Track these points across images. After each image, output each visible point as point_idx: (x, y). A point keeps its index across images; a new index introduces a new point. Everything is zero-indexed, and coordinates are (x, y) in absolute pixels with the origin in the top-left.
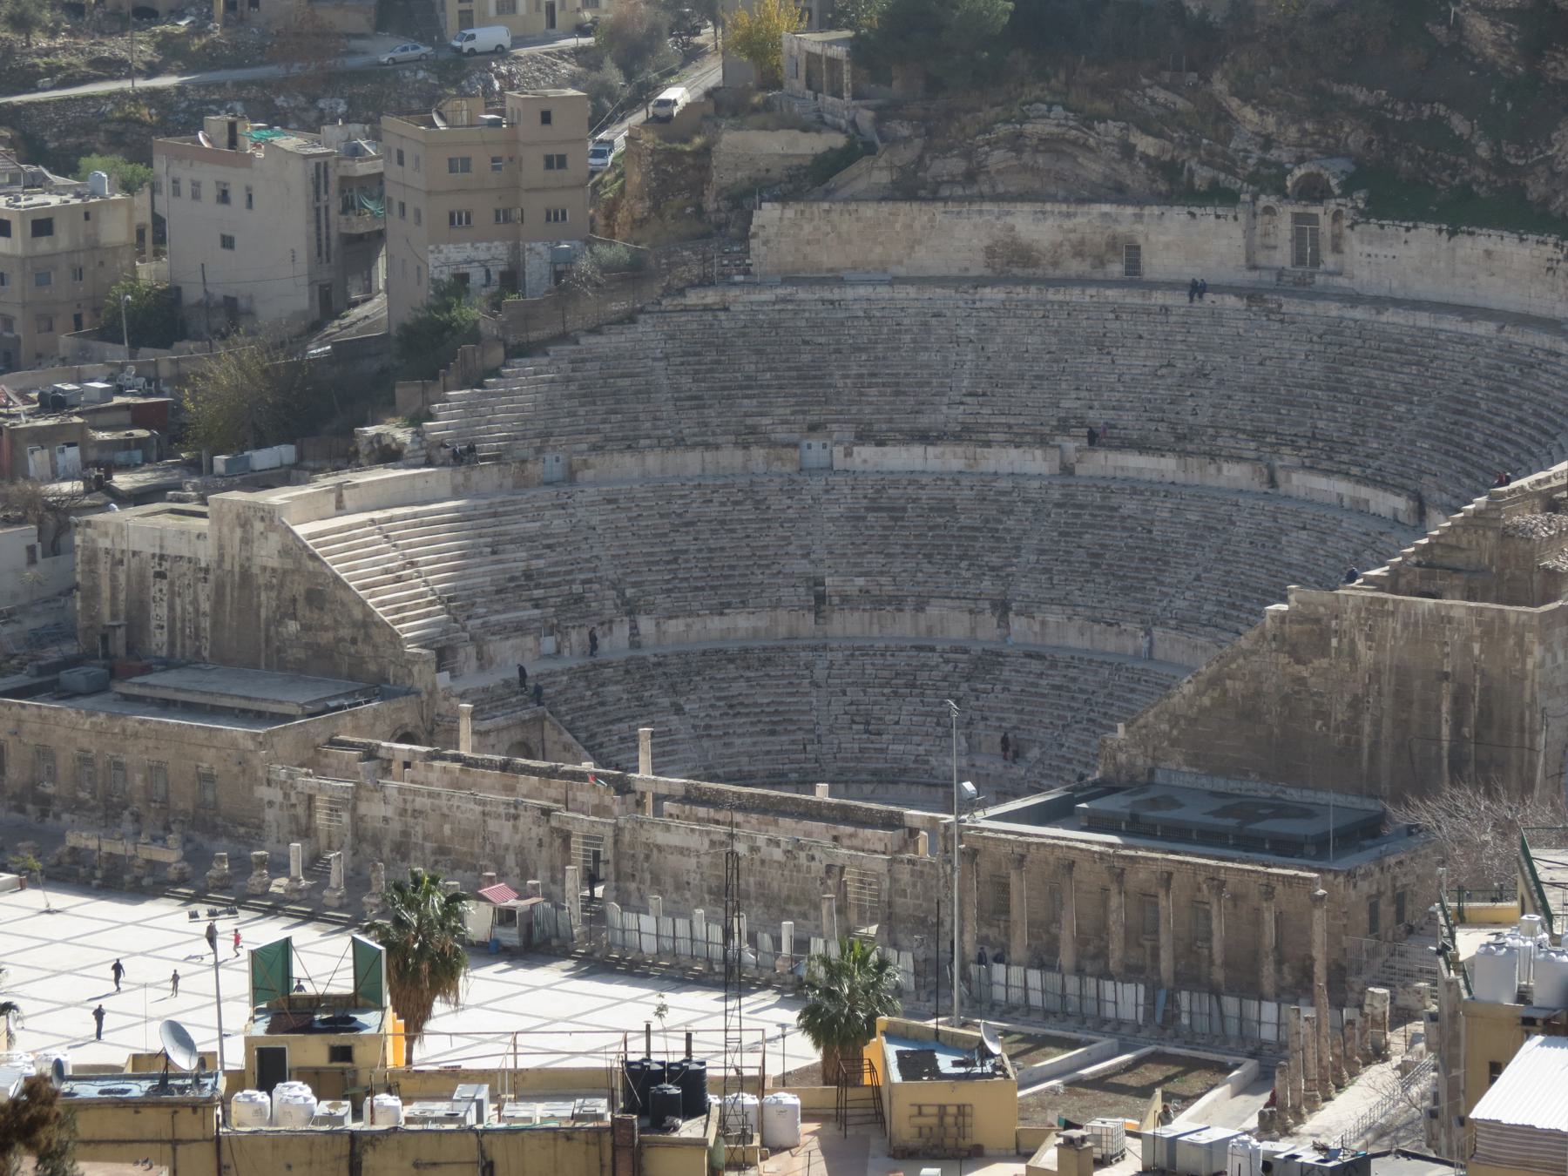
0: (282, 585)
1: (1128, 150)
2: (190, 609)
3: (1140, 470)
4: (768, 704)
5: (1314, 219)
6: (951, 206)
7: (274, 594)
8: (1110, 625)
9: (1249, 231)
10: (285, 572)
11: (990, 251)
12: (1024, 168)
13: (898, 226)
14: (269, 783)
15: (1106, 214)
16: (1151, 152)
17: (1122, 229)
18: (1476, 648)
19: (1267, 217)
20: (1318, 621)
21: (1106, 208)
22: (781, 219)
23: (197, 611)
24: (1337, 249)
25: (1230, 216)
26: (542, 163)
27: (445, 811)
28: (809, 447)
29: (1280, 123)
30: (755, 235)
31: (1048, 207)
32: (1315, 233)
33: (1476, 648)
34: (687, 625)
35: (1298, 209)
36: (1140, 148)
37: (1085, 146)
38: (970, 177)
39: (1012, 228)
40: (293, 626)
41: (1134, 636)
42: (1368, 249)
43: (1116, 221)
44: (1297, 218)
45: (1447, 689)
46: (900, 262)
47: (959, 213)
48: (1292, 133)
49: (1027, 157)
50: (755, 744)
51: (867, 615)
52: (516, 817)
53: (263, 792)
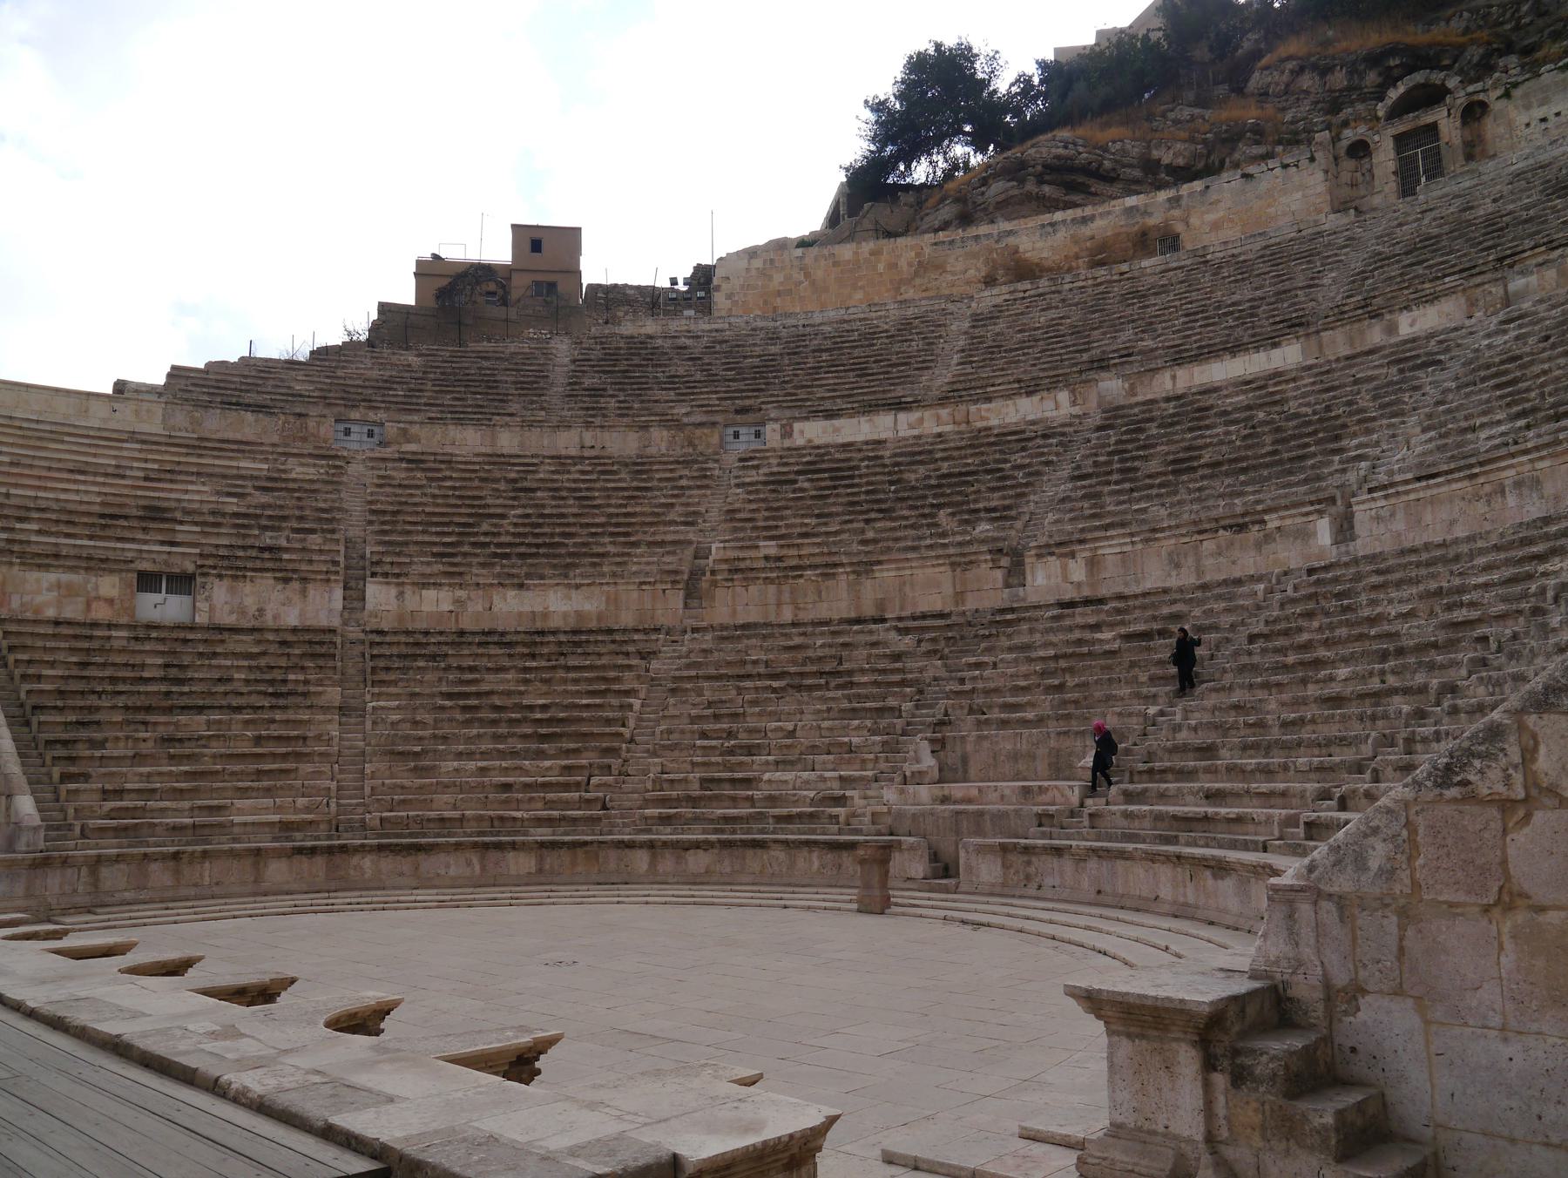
4: (544, 708)
5: (1433, 128)
8: (1241, 528)
12: (1029, 197)
13: (881, 267)
15: (1132, 208)
16: (1181, 161)
17: (1154, 220)
21: (1131, 201)
22: (748, 270)
25: (1304, 163)
28: (736, 435)
30: (718, 288)
31: (1058, 216)
34: (457, 601)
39: (1017, 252)
41: (1304, 535)
42: (1538, 113)
43: (1146, 213)
44: (1400, 140)
48: (1372, 78)
50: (483, 771)
51: (772, 589)
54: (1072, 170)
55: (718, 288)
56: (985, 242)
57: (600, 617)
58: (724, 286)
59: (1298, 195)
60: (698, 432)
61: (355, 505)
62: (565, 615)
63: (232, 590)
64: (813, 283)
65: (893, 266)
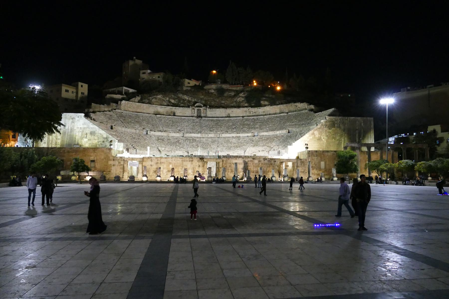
0: (83, 131)
1: (170, 102)
2: (55, 138)
7: (80, 133)
10: (85, 128)
14: (114, 160)
18: (362, 124)
20: (333, 122)
23: (57, 139)
27: (171, 161)
29: (191, 99)
33: (362, 124)
35: (198, 108)
40: (85, 140)
44: (198, 110)
45: (357, 131)
52: (192, 161)
53: (111, 162)
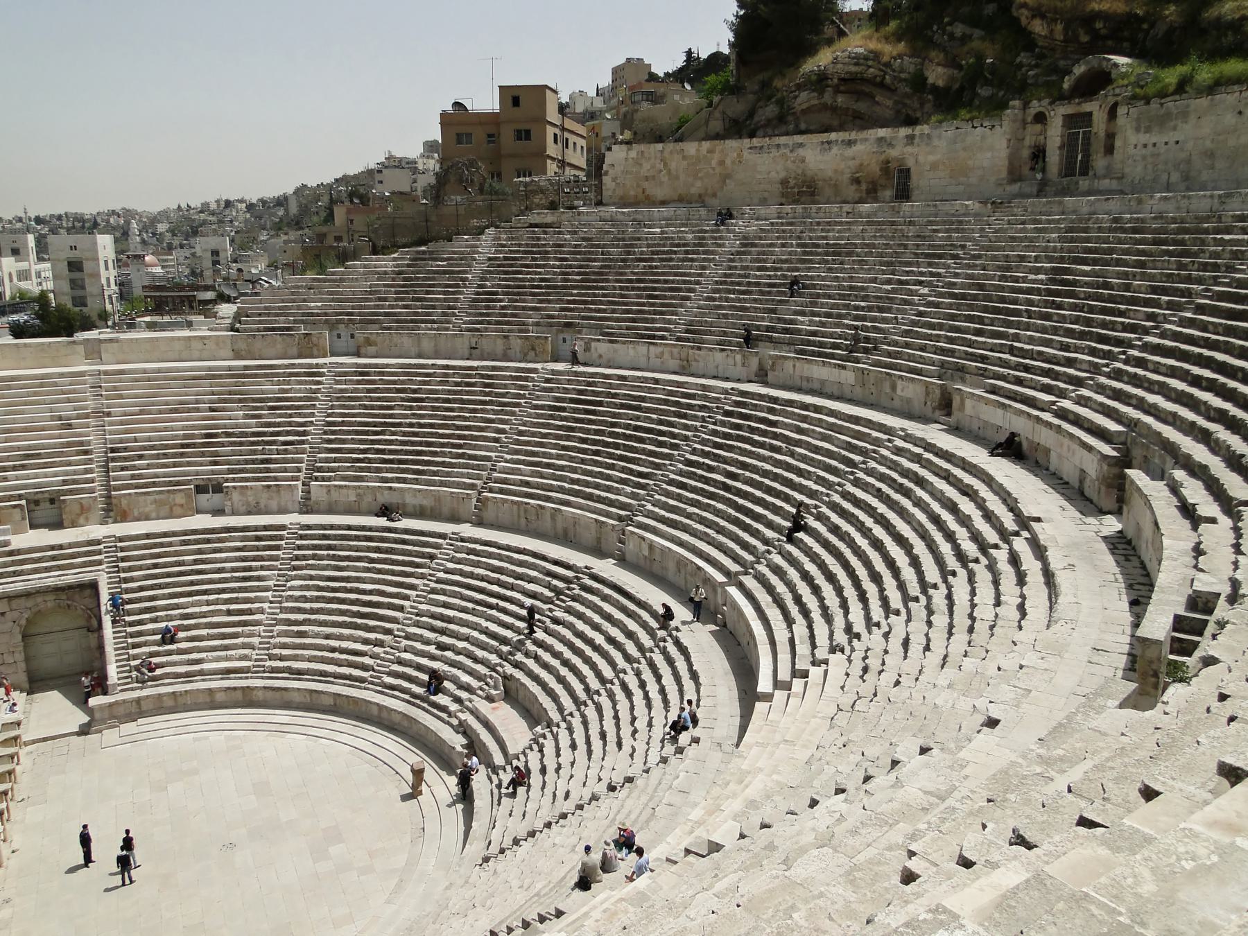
3: (823, 382)
6: (756, 142)
9: (1015, 141)
11: (784, 182)
12: (825, 107)
15: (881, 140)
16: (940, 83)
17: (894, 153)
19: (1038, 127)
21: (882, 132)
24: (1110, 150)
26: (512, 135)
28: (564, 340)
32: (1087, 137)
36: (930, 81)
37: (882, 85)
38: (781, 119)
42: (1144, 138)
43: (890, 145)
44: (1070, 121)
46: (714, 195)
47: (761, 148)
49: (828, 97)
51: (515, 507)
54: (864, 80)
55: (606, 173)
56: (783, 150)
57: (432, 509)
58: (611, 172)
59: (989, 155)
60: (537, 341)
61: (319, 416)
62: (414, 506)
63: (242, 494)
64: (669, 172)
65: (722, 163)
